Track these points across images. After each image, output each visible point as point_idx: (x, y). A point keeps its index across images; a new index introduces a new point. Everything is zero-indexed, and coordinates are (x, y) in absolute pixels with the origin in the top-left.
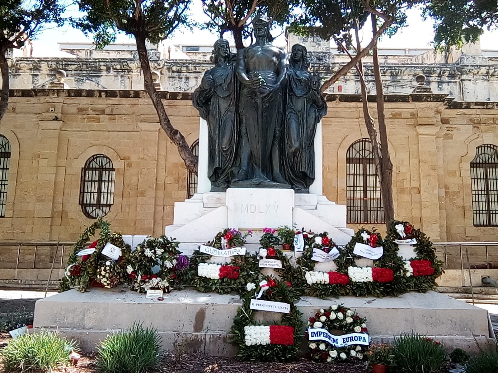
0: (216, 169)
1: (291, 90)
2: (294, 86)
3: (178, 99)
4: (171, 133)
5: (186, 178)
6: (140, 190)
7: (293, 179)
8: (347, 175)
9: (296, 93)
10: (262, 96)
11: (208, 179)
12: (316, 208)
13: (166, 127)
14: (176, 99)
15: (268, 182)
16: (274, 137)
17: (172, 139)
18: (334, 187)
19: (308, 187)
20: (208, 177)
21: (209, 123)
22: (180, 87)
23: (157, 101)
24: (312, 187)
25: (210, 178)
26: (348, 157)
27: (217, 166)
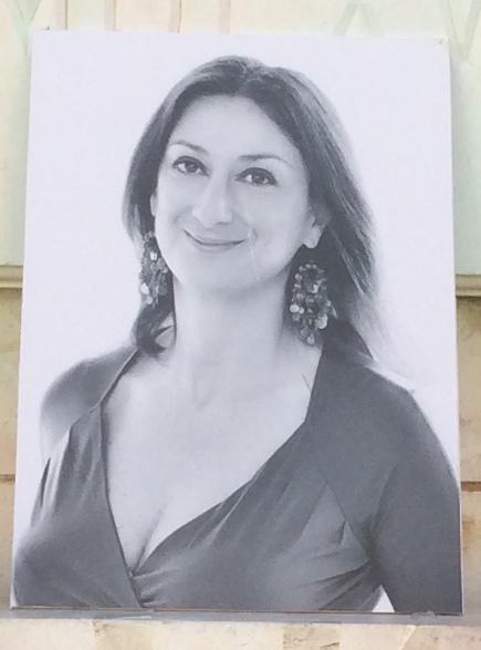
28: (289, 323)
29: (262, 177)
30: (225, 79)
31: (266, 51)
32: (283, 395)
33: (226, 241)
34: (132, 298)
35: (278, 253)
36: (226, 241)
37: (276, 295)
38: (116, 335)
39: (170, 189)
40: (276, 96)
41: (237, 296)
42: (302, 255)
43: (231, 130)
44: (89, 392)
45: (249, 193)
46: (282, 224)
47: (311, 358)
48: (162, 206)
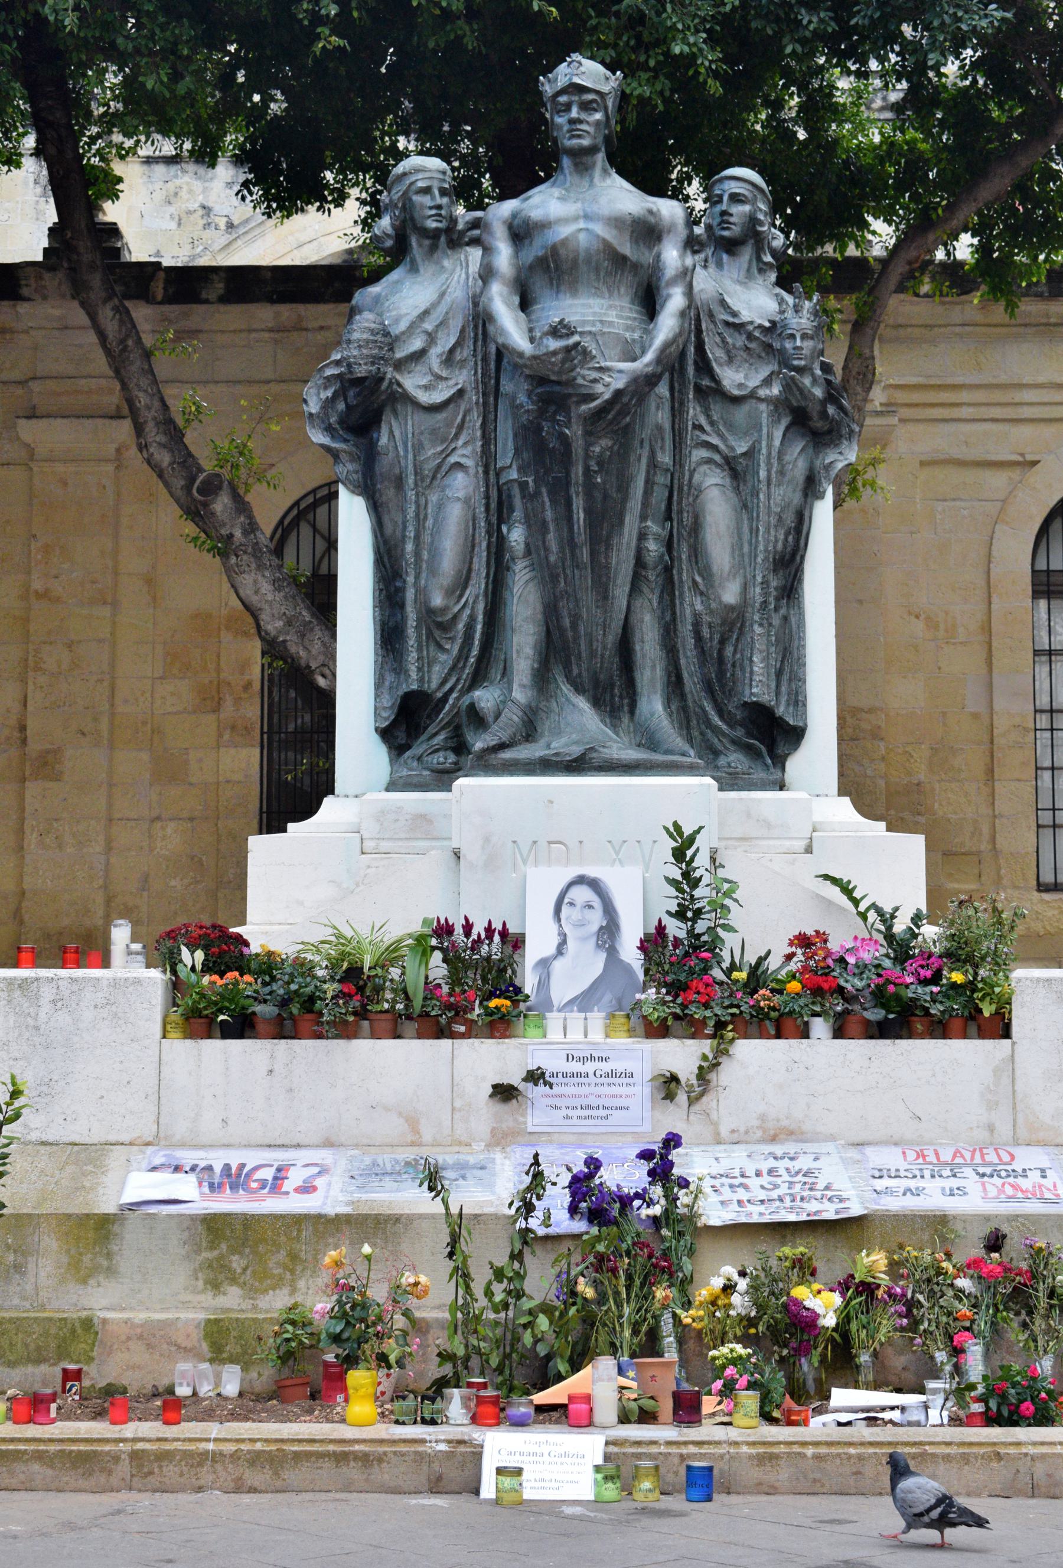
0: (408, 697)
1: (704, 366)
2: (714, 352)
3: (207, 301)
4: (188, 488)
5: (257, 686)
6: (34, 746)
7: (715, 730)
8: (1037, 653)
9: (726, 383)
10: (584, 408)
11: (376, 738)
12: (809, 850)
13: (164, 458)
14: (198, 300)
15: (620, 749)
16: (640, 563)
17: (196, 512)
18: (976, 716)
19: (780, 762)
20: (376, 729)
21: (376, 508)
22: (206, 209)
23: (122, 341)
24: (796, 765)
25: (385, 734)
26: (1041, 565)
27: (414, 687)
28: (598, 946)
29: (590, 907)
30: (581, 880)
31: (591, 872)
32: (597, 964)
33: (581, 924)
34: (555, 940)
35: (595, 928)
36: (581, 924)
37: (594, 939)
38: (552, 950)
39: (565, 910)
40: (594, 884)
41: (584, 939)
42: (601, 928)
43: (582, 894)
44: (544, 964)
45: (587, 911)
46: (596, 919)
47: (604, 955)
48: (564, 914)
